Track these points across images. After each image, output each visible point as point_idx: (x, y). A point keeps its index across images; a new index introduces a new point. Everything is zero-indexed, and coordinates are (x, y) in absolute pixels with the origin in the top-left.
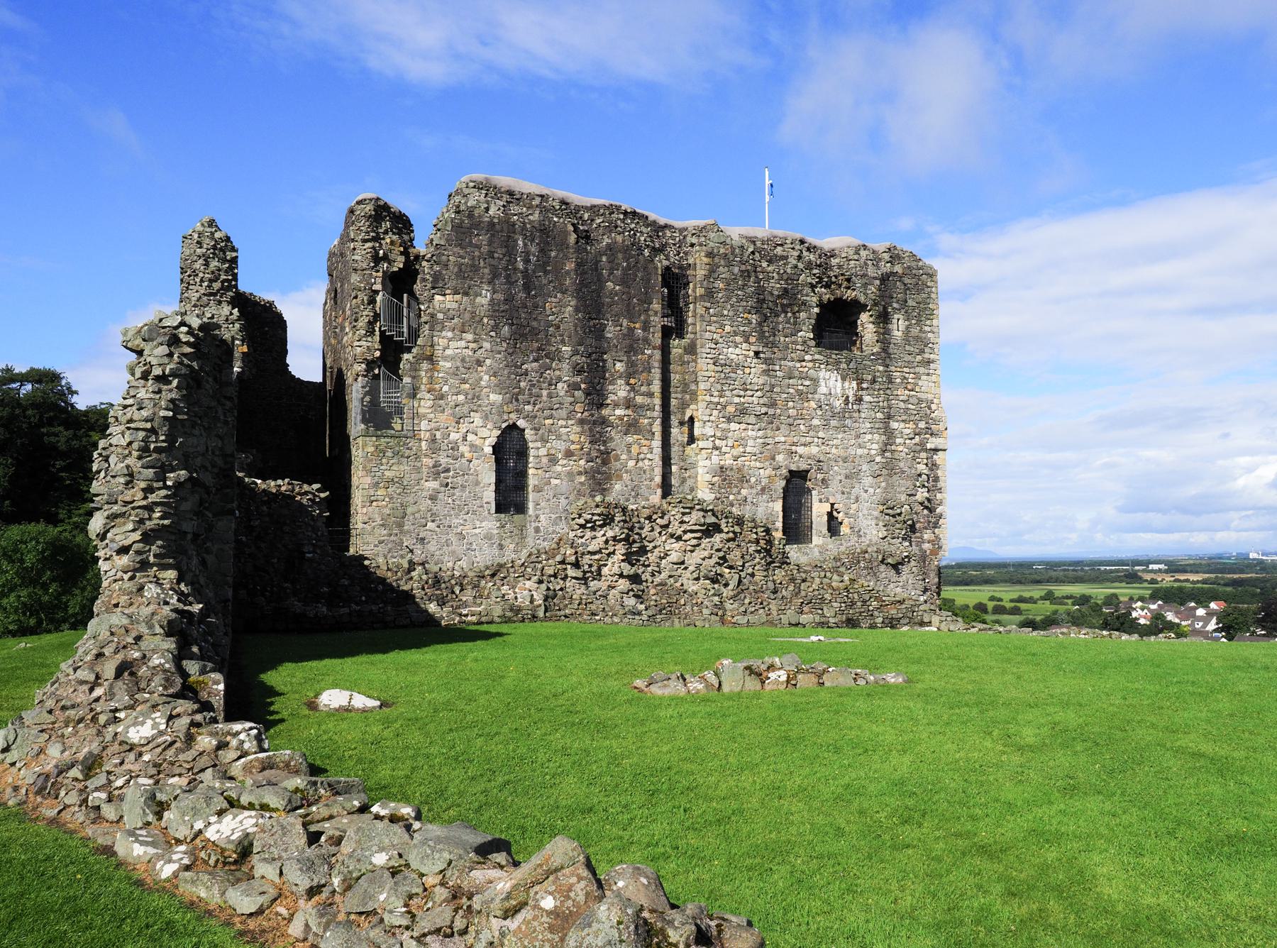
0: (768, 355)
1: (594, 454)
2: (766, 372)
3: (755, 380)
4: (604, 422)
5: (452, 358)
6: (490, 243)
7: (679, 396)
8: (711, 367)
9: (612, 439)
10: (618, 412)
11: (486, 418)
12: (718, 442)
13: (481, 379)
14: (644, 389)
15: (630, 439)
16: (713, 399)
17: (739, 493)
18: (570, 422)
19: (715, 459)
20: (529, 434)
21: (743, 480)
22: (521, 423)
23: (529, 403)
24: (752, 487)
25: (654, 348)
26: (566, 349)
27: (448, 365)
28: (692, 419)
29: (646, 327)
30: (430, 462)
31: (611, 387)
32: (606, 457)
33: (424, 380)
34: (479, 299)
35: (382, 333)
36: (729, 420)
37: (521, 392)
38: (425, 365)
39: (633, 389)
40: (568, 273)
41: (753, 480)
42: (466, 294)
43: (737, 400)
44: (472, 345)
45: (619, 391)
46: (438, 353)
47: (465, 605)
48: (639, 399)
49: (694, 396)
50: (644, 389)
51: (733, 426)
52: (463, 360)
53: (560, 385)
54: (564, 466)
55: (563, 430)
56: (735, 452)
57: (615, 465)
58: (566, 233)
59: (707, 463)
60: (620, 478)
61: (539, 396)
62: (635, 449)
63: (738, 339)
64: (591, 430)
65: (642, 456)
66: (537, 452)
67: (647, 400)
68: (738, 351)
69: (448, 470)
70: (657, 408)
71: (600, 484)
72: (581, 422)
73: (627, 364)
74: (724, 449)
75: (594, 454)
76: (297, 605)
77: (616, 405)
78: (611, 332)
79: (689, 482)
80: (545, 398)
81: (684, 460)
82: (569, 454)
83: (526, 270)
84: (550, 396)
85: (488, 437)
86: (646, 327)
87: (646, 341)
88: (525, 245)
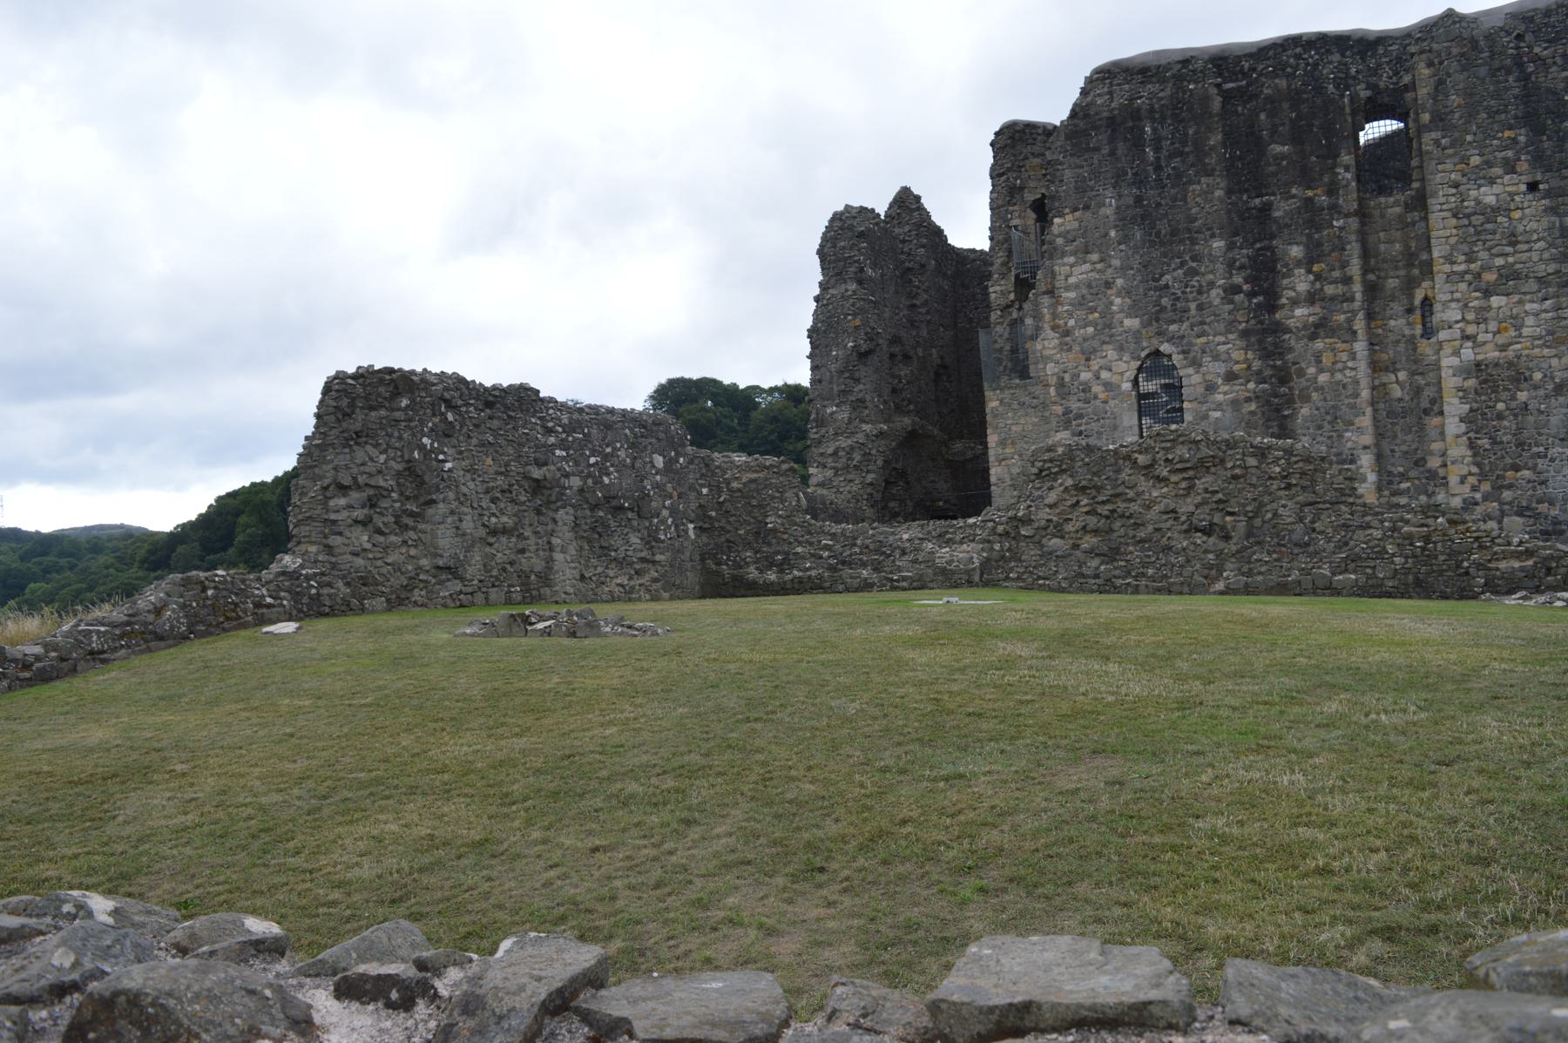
0: (1555, 183)
1: (1268, 372)
2: (1552, 210)
3: (1533, 225)
4: (1278, 329)
5: (1077, 287)
6: (1112, 140)
7: (1402, 273)
8: (1454, 221)
9: (1291, 349)
10: (1298, 312)
11: (1121, 349)
12: (1471, 329)
13: (1112, 303)
14: (1336, 274)
15: (1319, 345)
16: (1456, 268)
17: (1513, 398)
18: (1231, 337)
19: (1468, 353)
20: (1177, 359)
21: (1519, 377)
22: (1165, 348)
23: (1174, 322)
24: (1536, 387)
25: (1347, 216)
26: (1218, 244)
27: (1072, 295)
28: (1427, 303)
29: (1332, 191)
30: (1059, 409)
31: (1285, 282)
32: (1283, 377)
33: (1047, 317)
34: (1103, 211)
35: (1017, 276)
36: (1487, 294)
37: (1163, 309)
38: (1046, 300)
39: (1318, 277)
40: (1212, 148)
41: (1538, 376)
42: (1086, 208)
43: (1499, 261)
44: (1098, 266)
45: (1301, 283)
46: (1060, 283)
47: (899, 569)
48: (1330, 290)
49: (1428, 269)
50: (1336, 274)
51: (1496, 301)
52: (1089, 286)
53: (1214, 293)
54: (1225, 393)
55: (1222, 348)
56: (1501, 339)
57: (1299, 384)
58: (1206, 99)
59: (1455, 361)
60: (1306, 398)
61: (1187, 310)
62: (1327, 359)
63: (1498, 171)
64: (1260, 342)
65: (1339, 366)
66: (1192, 380)
67: (1340, 289)
68: (1497, 189)
69: (1080, 416)
70: (1358, 296)
71: (1278, 411)
72: (1245, 334)
73: (1307, 247)
74: (1480, 338)
75: (1268, 372)
76: (752, 573)
77: (1295, 303)
78: (1281, 209)
79: (1429, 392)
80: (1193, 312)
81: (1415, 362)
82: (1230, 377)
83: (1158, 159)
84: (1200, 308)
85: (1122, 369)
86: (1332, 191)
87: (1334, 208)
88: (1154, 130)
